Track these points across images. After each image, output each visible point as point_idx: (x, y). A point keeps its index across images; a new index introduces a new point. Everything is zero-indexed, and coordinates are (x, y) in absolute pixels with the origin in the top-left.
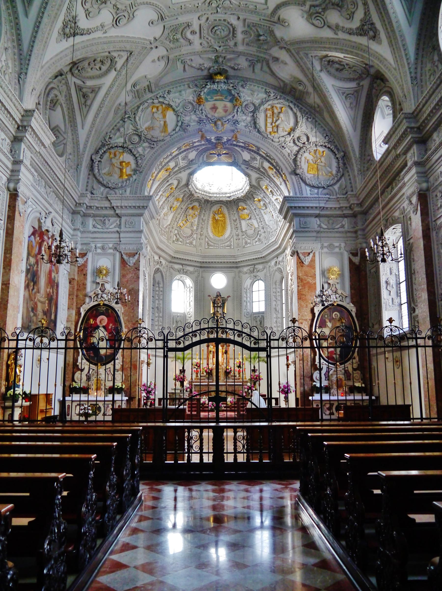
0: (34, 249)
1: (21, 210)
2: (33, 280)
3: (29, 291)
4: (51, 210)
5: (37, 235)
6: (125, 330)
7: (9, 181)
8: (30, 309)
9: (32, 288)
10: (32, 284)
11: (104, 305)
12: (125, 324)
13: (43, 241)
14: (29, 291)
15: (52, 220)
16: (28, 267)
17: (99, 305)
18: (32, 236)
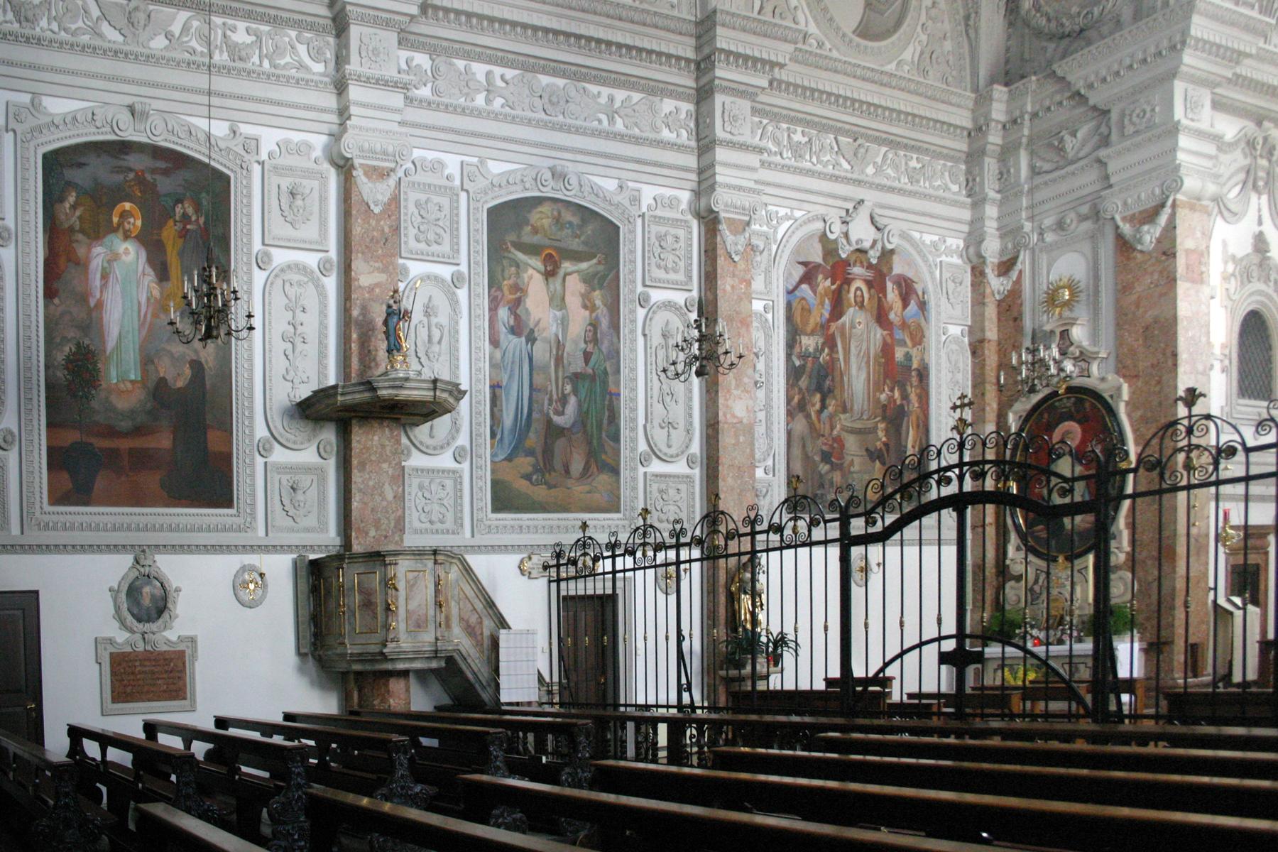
0: (815, 313)
1: (731, 249)
2: (819, 388)
3: (808, 416)
4: (859, 193)
5: (820, 277)
6: (1133, 449)
7: (697, 194)
8: (817, 458)
9: (818, 406)
10: (818, 396)
11: (1070, 390)
12: (1135, 431)
13: (848, 282)
14: (808, 416)
15: (872, 218)
16: (797, 363)
17: (1055, 394)
18: (804, 286)
